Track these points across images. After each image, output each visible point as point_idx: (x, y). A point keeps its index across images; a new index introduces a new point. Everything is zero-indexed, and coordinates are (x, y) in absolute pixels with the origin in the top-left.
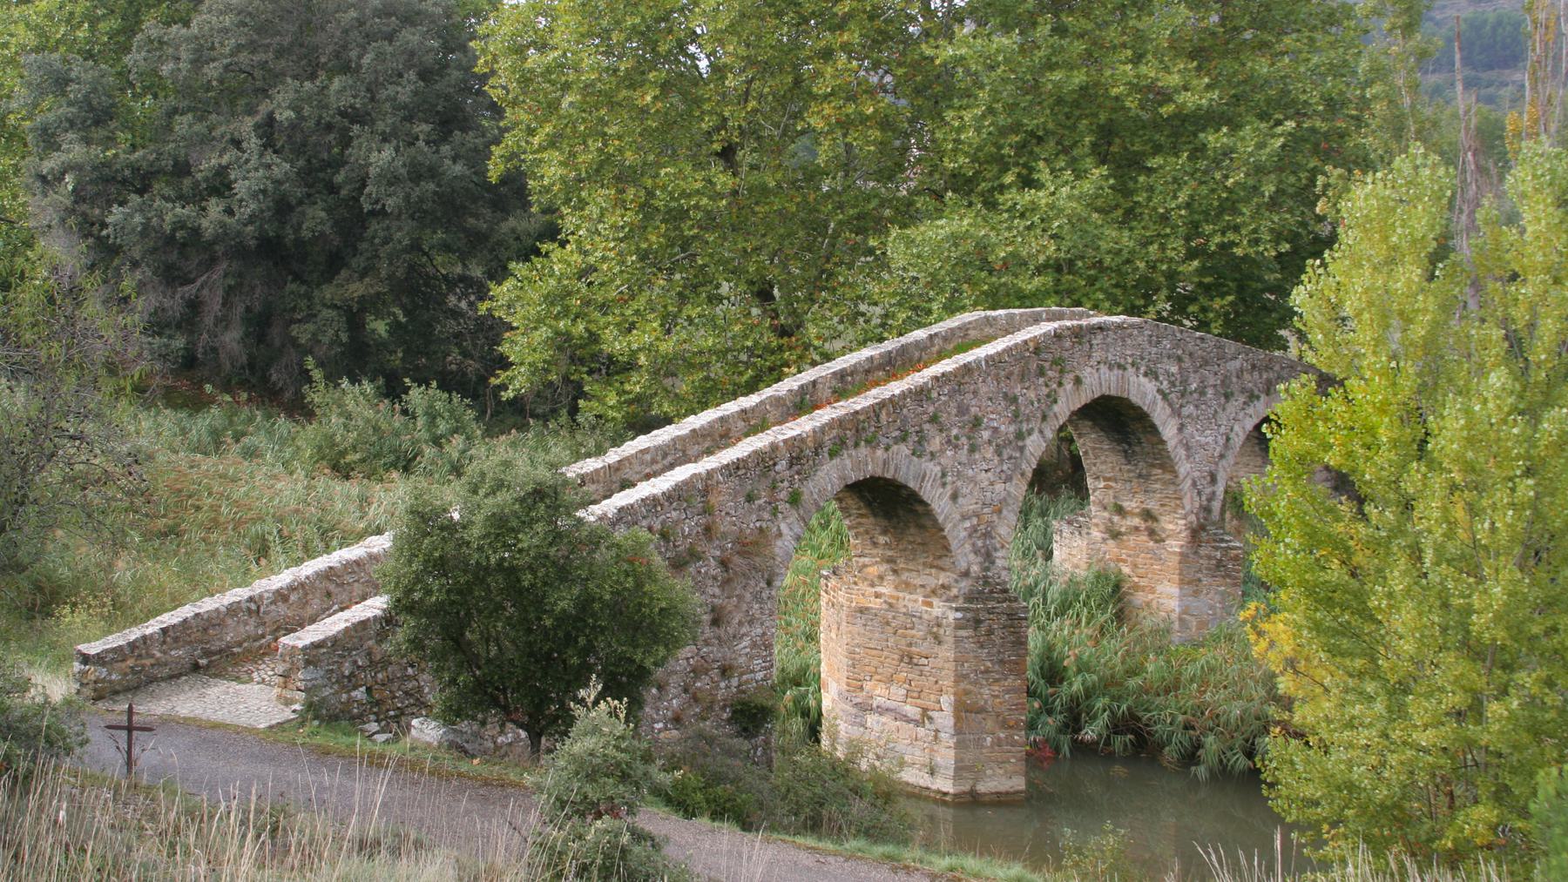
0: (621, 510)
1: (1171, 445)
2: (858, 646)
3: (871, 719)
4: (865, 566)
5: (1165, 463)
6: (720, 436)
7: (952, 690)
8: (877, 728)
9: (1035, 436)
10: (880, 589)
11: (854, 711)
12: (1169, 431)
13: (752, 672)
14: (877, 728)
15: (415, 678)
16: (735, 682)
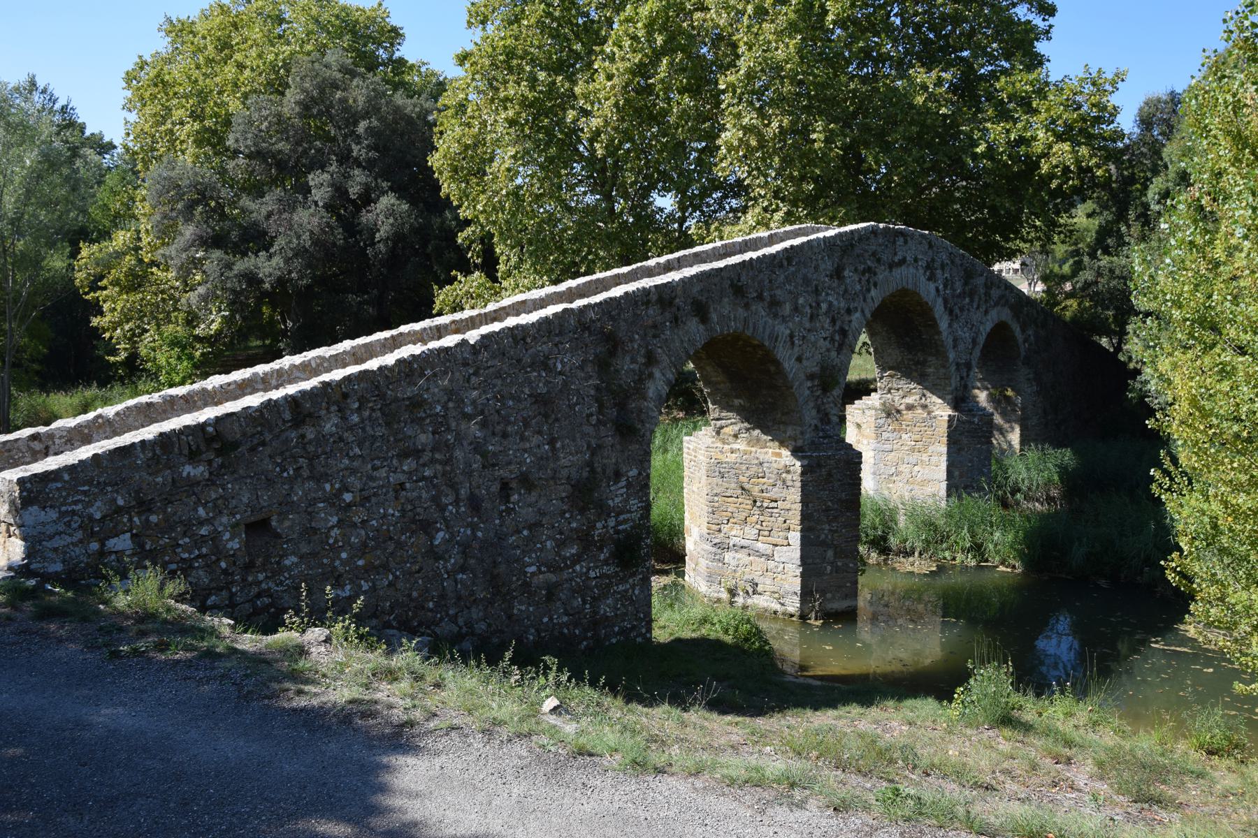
1: (945, 334)
2: (716, 495)
3: (728, 556)
4: (722, 428)
5: (936, 349)
7: (799, 528)
8: (733, 563)
9: (858, 315)
10: (735, 446)
11: (714, 550)
12: (943, 325)
13: (630, 512)
14: (733, 563)
15: (208, 521)
16: (612, 522)
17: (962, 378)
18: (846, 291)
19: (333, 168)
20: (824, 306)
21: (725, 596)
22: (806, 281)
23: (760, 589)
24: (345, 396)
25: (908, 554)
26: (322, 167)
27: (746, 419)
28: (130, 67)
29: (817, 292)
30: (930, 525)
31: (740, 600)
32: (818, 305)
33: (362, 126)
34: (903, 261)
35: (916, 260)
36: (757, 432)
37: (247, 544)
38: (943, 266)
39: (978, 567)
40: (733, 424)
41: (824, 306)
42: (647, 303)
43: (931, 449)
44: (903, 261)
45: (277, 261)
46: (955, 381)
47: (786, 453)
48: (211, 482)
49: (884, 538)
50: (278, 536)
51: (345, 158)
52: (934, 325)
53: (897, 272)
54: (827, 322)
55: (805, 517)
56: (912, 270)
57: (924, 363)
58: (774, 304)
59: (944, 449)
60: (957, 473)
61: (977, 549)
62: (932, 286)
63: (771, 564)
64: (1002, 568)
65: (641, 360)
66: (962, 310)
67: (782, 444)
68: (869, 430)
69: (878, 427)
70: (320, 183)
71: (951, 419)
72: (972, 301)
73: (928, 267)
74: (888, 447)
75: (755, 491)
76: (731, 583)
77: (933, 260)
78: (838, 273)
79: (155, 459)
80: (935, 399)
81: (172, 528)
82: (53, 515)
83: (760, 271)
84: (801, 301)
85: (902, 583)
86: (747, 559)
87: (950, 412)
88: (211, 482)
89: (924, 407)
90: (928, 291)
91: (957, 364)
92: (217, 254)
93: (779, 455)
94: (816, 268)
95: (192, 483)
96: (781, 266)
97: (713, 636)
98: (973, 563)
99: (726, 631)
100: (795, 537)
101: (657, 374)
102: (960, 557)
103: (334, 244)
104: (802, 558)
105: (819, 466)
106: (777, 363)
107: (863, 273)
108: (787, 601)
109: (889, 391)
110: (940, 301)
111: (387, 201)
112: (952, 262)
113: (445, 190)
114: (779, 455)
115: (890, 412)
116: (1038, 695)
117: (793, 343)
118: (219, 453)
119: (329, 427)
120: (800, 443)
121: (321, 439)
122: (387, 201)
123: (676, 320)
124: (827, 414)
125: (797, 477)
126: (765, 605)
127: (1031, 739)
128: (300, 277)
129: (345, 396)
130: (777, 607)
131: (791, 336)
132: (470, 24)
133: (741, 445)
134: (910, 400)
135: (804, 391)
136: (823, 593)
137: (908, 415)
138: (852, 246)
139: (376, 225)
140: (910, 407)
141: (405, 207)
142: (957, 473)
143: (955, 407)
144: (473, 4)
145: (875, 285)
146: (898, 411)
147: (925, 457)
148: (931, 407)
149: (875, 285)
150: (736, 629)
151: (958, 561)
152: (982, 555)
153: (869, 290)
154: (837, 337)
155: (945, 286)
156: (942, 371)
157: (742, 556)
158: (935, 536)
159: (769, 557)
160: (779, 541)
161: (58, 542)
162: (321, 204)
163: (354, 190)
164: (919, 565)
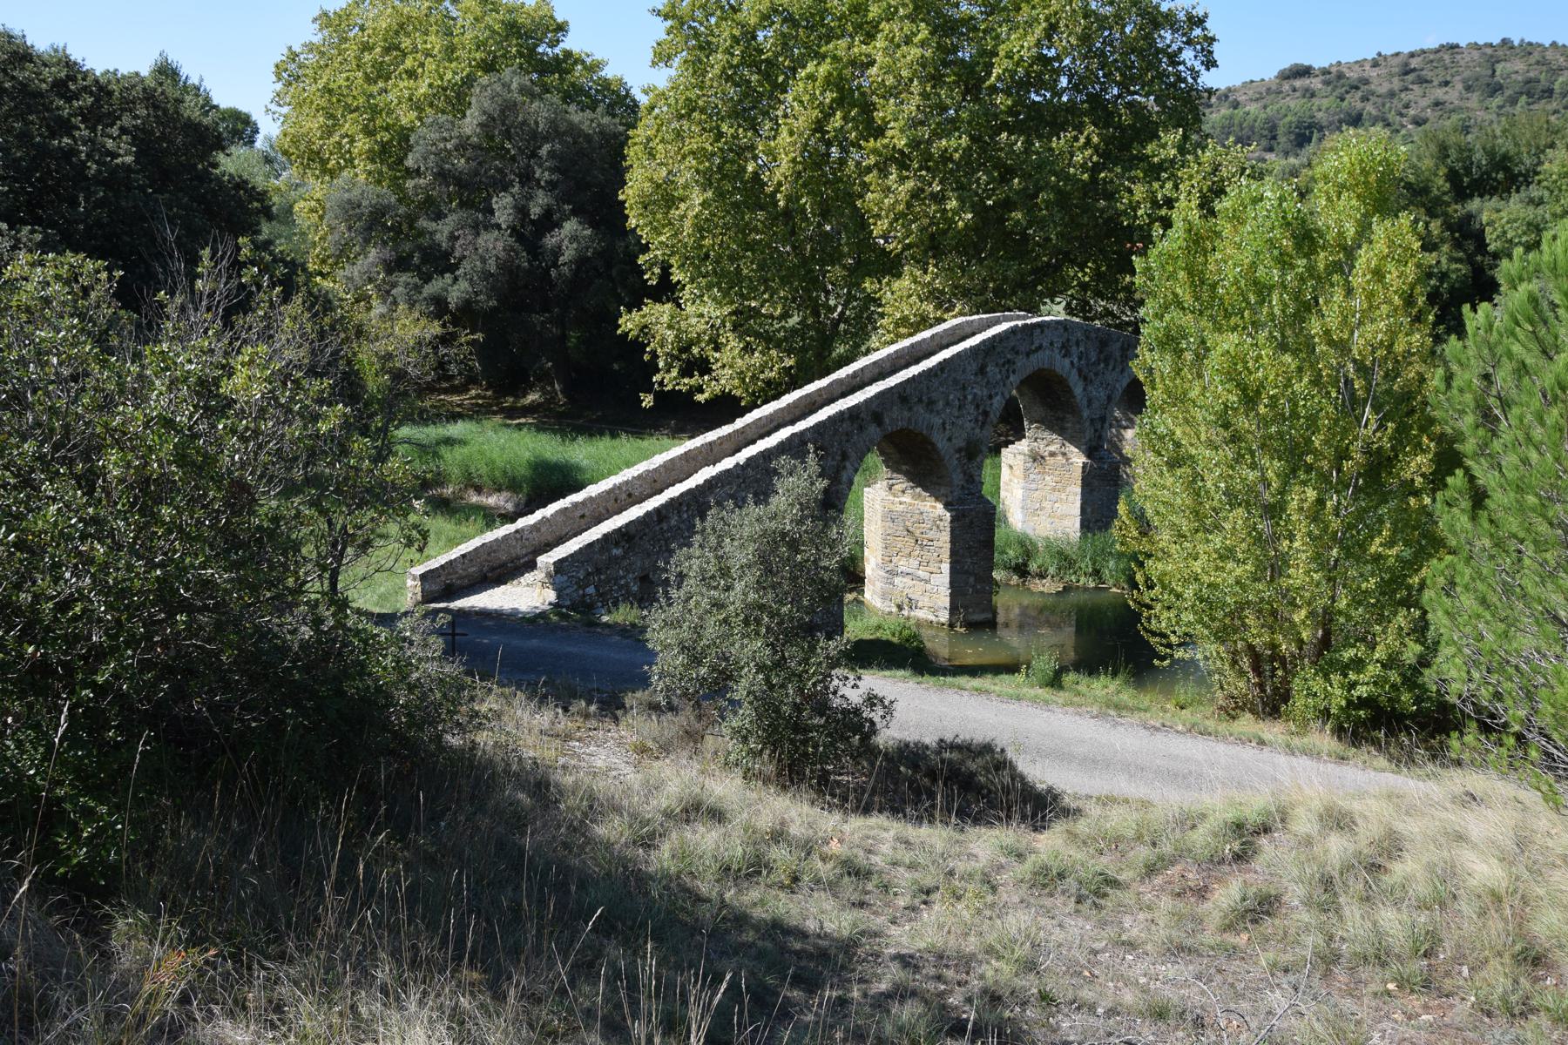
0: (748, 459)
1: (1079, 397)
3: (897, 580)
5: (1075, 410)
6: (810, 405)
8: (901, 585)
9: (998, 398)
10: (903, 499)
12: (1078, 390)
15: (624, 577)
17: (1096, 431)
18: (988, 382)
19: (516, 189)
20: (970, 397)
21: (894, 609)
22: (956, 382)
23: (920, 605)
24: (681, 504)
25: (1042, 576)
26: (505, 189)
27: (910, 479)
28: (279, 58)
29: (964, 388)
30: (1061, 554)
31: (905, 613)
32: (965, 397)
33: (546, 148)
34: (1040, 347)
35: (1052, 344)
36: (919, 490)
37: (640, 588)
38: (1078, 344)
39: (1096, 588)
40: (901, 483)
41: (970, 397)
42: (842, 421)
43: (1068, 489)
44: (1040, 347)
45: (463, 285)
46: (1089, 434)
47: (940, 506)
48: (623, 558)
49: (1025, 565)
50: (652, 583)
51: (526, 178)
52: (1069, 391)
53: (1033, 358)
54: (972, 409)
55: (953, 553)
56: (1047, 352)
57: (1063, 419)
58: (931, 403)
59: (1079, 490)
60: (1089, 510)
61: (1097, 573)
62: (1067, 361)
63: (928, 587)
64: (1114, 590)
65: (838, 458)
66: (1096, 374)
67: (937, 499)
68: (1019, 471)
69: (1026, 470)
70: (503, 207)
71: (1085, 465)
72: (1107, 365)
73: (1063, 346)
74: (1033, 486)
75: (917, 533)
76: (899, 601)
77: (1068, 340)
78: (982, 371)
79: (602, 547)
80: (1072, 448)
81: (609, 582)
82: (565, 578)
83: (920, 383)
84: (951, 397)
85: (1039, 601)
86: (911, 583)
87: (1084, 459)
88: (623, 558)
89: (1064, 454)
90: (1063, 366)
91: (1092, 420)
92: (404, 278)
93: (935, 507)
94: (964, 371)
95: (616, 557)
96: (936, 375)
97: (884, 638)
98: (1092, 585)
99: (893, 635)
100: (946, 567)
101: (848, 464)
102: (1083, 579)
103: (519, 266)
104: (951, 583)
105: (964, 516)
106: (933, 444)
107: (1003, 365)
108: (939, 614)
109: (1036, 440)
110: (1074, 372)
111: (570, 226)
112: (1087, 338)
113: (632, 222)
114: (935, 507)
115: (1036, 458)
116: (1090, 675)
117: (945, 429)
118: (627, 541)
119: (673, 522)
120: (950, 499)
121: (670, 529)
122: (570, 226)
123: (861, 428)
124: (971, 476)
125: (947, 524)
126: (924, 616)
127: (1061, 693)
128: (487, 302)
129: (681, 504)
130: (932, 618)
131: (944, 424)
132: (654, 64)
133: (907, 499)
134: (1052, 448)
135: (953, 462)
136: (966, 608)
137: (1050, 461)
138: (994, 347)
139: (560, 247)
140: (1052, 454)
141: (588, 232)
142: (1089, 510)
143: (1089, 457)
144: (659, 44)
145: (1014, 372)
146: (1043, 457)
147: (1063, 496)
148: (1069, 455)
149: (1014, 372)
150: (901, 633)
151: (1081, 583)
152: (1100, 578)
153: (1008, 377)
154: (980, 418)
155: (1080, 359)
156: (1078, 426)
157: (907, 580)
158: (1065, 561)
159: (927, 582)
160: (935, 570)
161: (568, 591)
162: (504, 226)
163: (535, 211)
164: (1048, 586)
